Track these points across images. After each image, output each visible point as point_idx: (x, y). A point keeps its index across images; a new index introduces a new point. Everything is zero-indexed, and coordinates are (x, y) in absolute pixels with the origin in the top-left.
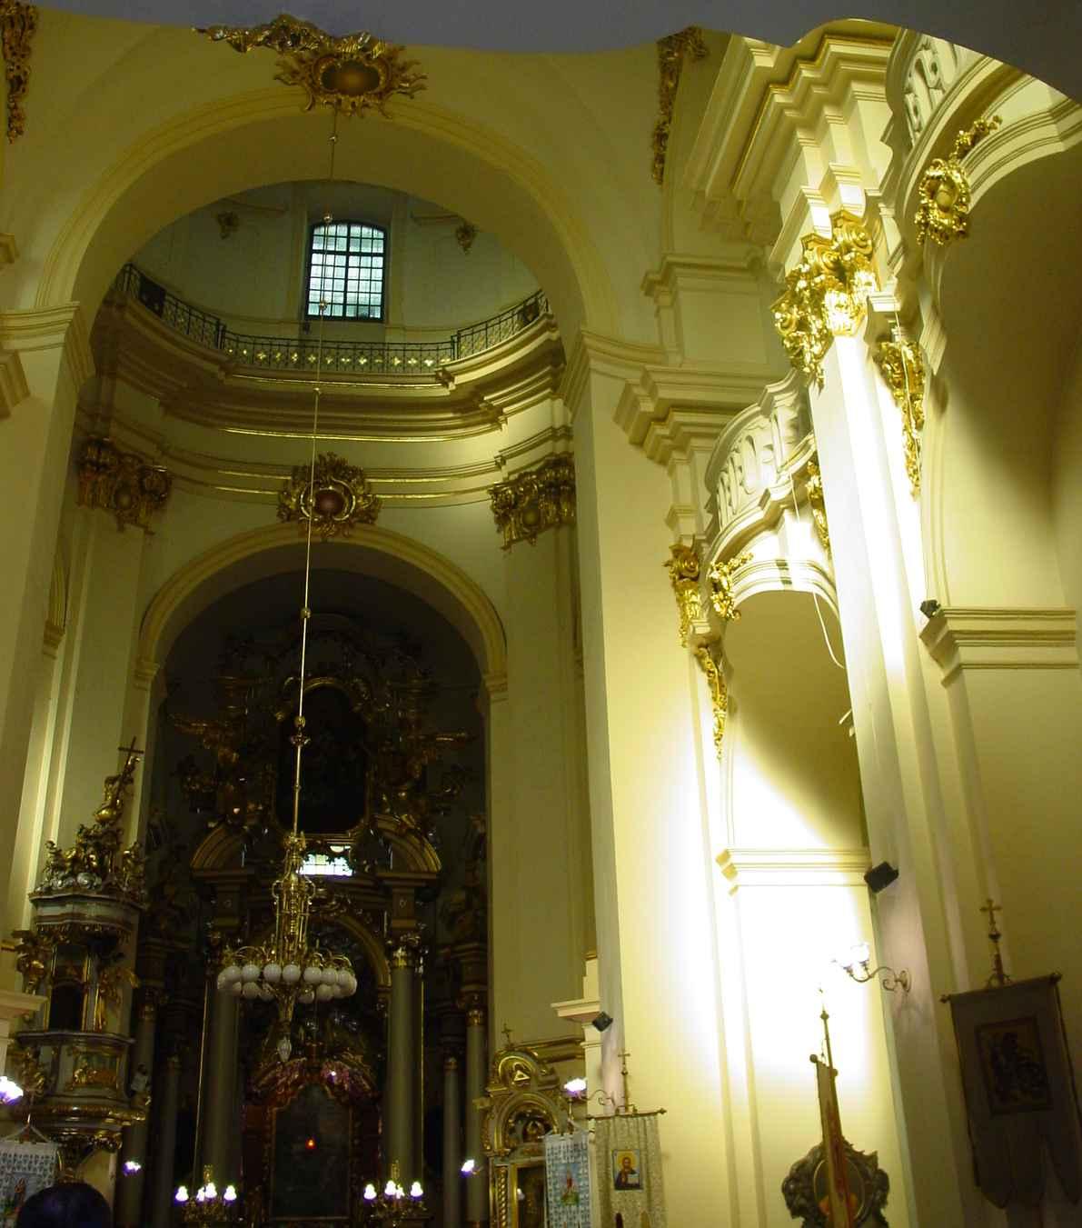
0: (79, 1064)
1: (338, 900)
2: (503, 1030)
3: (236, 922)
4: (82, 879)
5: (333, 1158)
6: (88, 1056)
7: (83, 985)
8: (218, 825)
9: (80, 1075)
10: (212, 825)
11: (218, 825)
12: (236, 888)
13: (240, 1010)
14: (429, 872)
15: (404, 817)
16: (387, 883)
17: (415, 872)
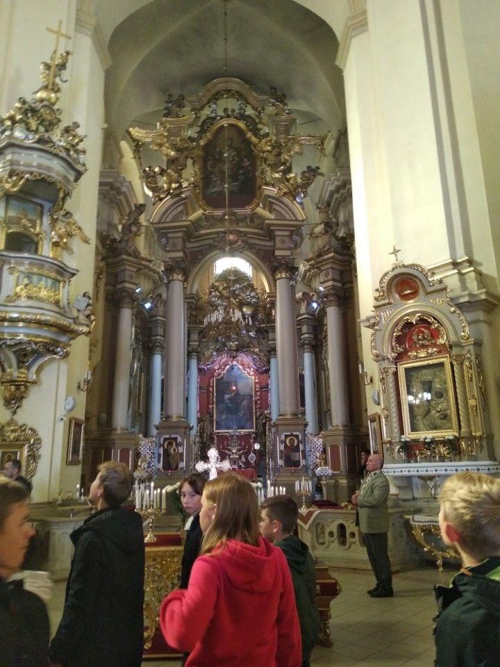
0: (20, 282)
1: (243, 241)
2: (392, 251)
3: (180, 254)
4: (19, 133)
5: (246, 401)
6: (29, 275)
7: (37, 235)
8: (167, 195)
9: (22, 290)
10: (162, 196)
11: (167, 195)
12: (180, 234)
13: (187, 309)
14: (297, 220)
15: (280, 186)
16: (272, 228)
17: (289, 220)
